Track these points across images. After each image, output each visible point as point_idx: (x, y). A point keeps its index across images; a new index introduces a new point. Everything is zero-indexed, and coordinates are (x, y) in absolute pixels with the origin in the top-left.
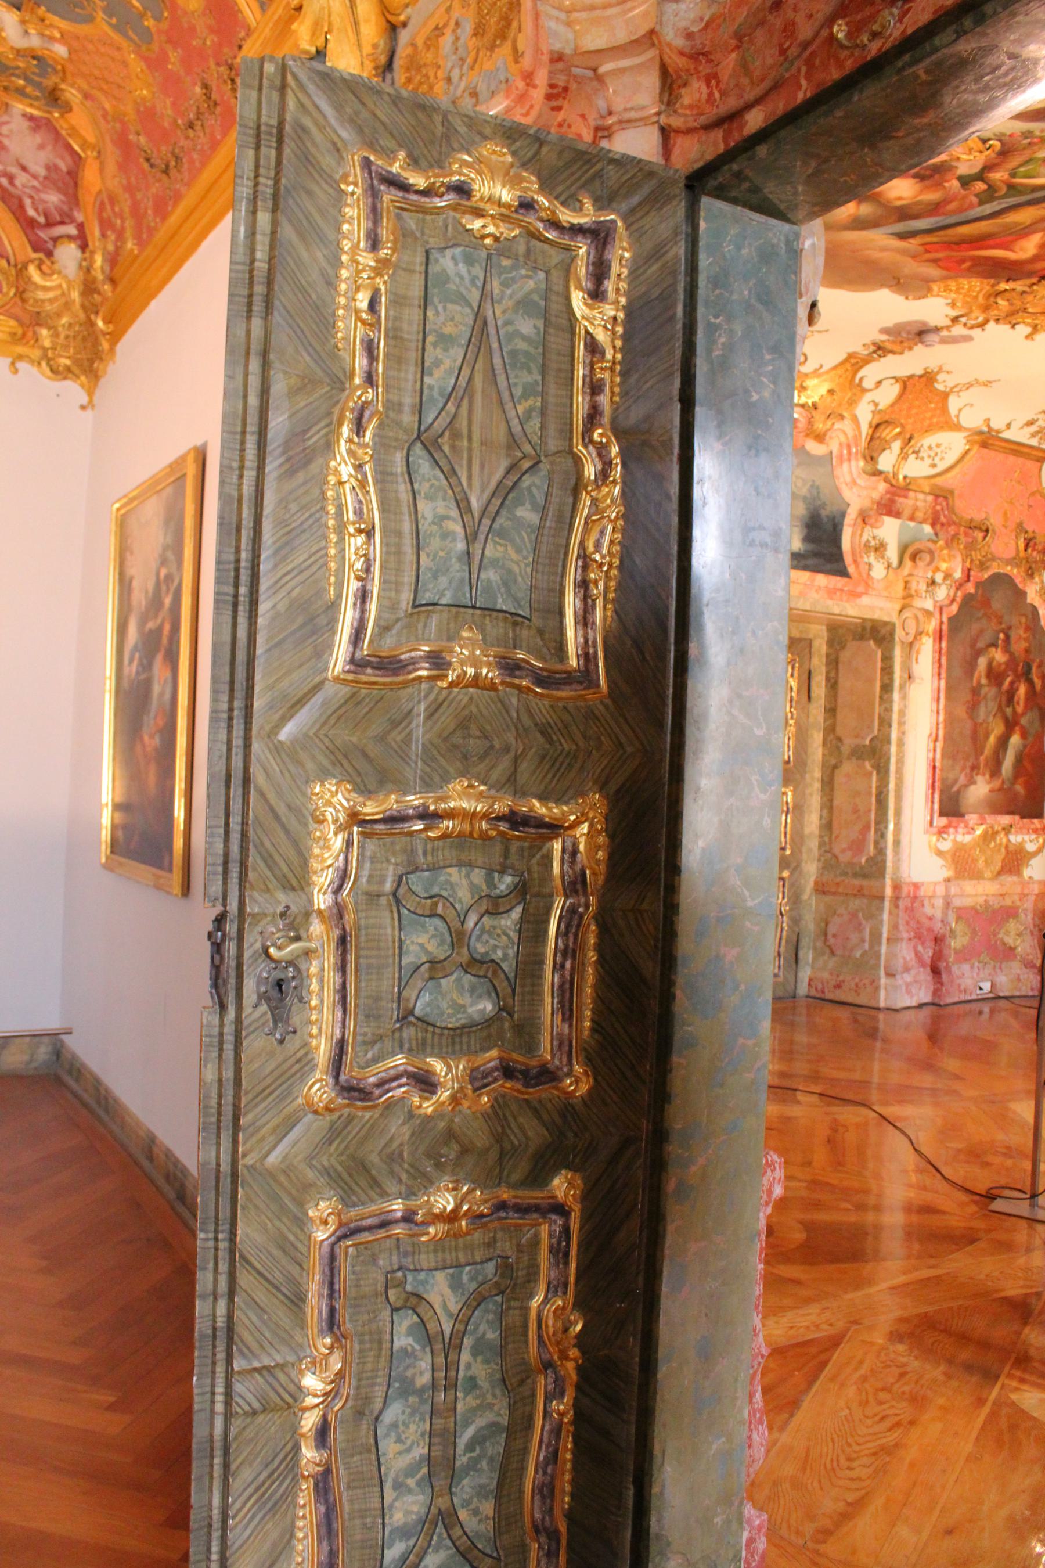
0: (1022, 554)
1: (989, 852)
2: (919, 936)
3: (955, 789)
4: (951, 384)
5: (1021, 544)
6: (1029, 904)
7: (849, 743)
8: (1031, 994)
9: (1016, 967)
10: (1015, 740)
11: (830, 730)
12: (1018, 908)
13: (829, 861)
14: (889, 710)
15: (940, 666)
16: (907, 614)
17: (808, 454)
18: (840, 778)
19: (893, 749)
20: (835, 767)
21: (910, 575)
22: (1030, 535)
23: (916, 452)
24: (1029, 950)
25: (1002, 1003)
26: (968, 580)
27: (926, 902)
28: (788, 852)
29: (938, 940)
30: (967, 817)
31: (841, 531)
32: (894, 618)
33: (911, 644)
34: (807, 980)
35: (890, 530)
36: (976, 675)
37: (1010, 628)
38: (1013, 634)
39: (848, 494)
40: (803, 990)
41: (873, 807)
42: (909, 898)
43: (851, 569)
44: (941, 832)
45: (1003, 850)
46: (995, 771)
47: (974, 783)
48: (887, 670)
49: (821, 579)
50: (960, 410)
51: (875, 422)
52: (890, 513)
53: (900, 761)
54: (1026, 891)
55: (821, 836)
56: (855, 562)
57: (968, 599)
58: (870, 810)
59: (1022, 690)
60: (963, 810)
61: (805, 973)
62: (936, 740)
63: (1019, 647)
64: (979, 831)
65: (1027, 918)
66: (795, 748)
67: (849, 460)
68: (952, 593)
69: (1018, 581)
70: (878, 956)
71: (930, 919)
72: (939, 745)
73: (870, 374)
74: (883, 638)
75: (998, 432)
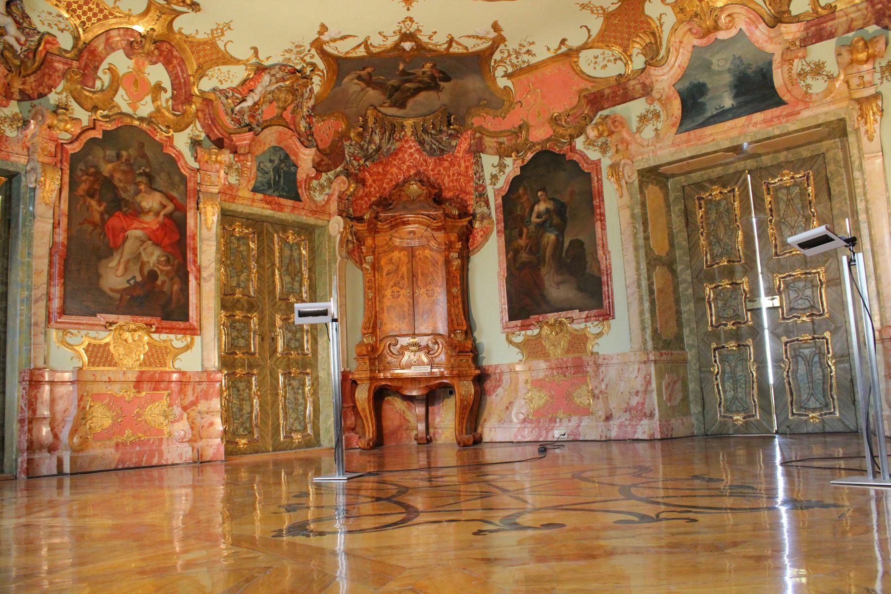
17: (723, 41)
31: (772, 75)
32: (843, 116)
39: (769, 48)
43: (785, 98)
49: (758, 117)
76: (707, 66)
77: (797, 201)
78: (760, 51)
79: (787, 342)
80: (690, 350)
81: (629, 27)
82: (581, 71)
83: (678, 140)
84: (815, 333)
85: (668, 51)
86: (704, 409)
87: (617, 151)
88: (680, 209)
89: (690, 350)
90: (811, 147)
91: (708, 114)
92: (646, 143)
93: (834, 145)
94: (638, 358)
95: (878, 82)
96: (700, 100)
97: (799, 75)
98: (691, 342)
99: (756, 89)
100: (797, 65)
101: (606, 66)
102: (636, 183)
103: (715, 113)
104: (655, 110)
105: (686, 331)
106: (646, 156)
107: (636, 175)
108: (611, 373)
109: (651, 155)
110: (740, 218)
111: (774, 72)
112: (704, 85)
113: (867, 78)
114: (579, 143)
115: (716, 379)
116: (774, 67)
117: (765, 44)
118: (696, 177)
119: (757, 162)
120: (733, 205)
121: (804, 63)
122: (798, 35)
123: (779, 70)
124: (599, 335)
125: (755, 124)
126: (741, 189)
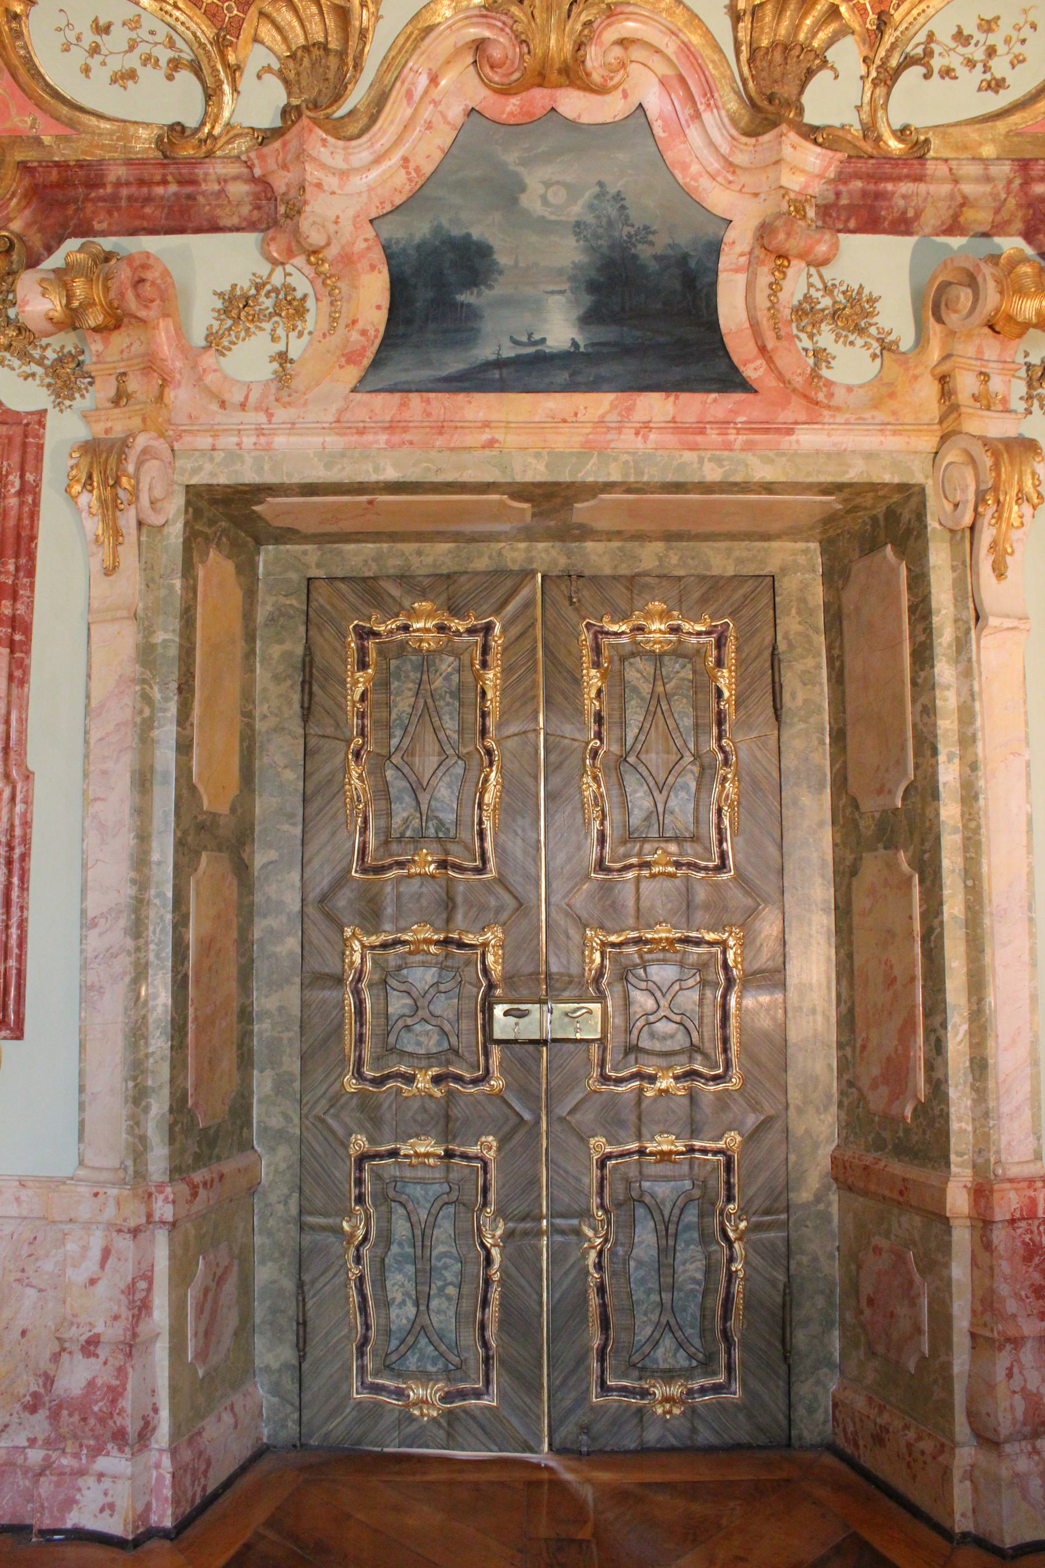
16: (952, 455)
17: (573, 125)
20: (854, 872)
21: (946, 357)
31: (714, 284)
32: (918, 478)
35: (878, 266)
39: (719, 199)
41: (919, 971)
43: (753, 371)
48: (921, 611)
49: (655, 406)
55: (840, 1046)
58: (913, 979)
67: (697, 115)
76: (506, 193)
78: (690, 198)
79: (609, 1157)
80: (272, 1150)
82: (29, 61)
83: (360, 414)
84: (694, 1133)
85: (379, 101)
86: (302, 1359)
87: (120, 398)
88: (287, 656)
89: (272, 1150)
90: (740, 549)
91: (486, 352)
92: (238, 397)
93: (802, 560)
94: (110, 1212)
95: (1021, 406)
96: (463, 297)
97: (799, 312)
98: (276, 1122)
99: (657, 316)
100: (797, 284)
101: (131, 75)
102: (176, 532)
103: (509, 352)
104: (289, 289)
105: (262, 1083)
106: (229, 441)
107: (179, 501)
110: (499, 726)
111: (722, 277)
112: (484, 251)
113: (996, 384)
115: (358, 1260)
116: (725, 261)
117: (705, 182)
118: (358, 556)
119: (569, 555)
120: (478, 677)
121: (815, 280)
122: (816, 188)
123: (741, 279)
125: (644, 428)
126: (514, 631)
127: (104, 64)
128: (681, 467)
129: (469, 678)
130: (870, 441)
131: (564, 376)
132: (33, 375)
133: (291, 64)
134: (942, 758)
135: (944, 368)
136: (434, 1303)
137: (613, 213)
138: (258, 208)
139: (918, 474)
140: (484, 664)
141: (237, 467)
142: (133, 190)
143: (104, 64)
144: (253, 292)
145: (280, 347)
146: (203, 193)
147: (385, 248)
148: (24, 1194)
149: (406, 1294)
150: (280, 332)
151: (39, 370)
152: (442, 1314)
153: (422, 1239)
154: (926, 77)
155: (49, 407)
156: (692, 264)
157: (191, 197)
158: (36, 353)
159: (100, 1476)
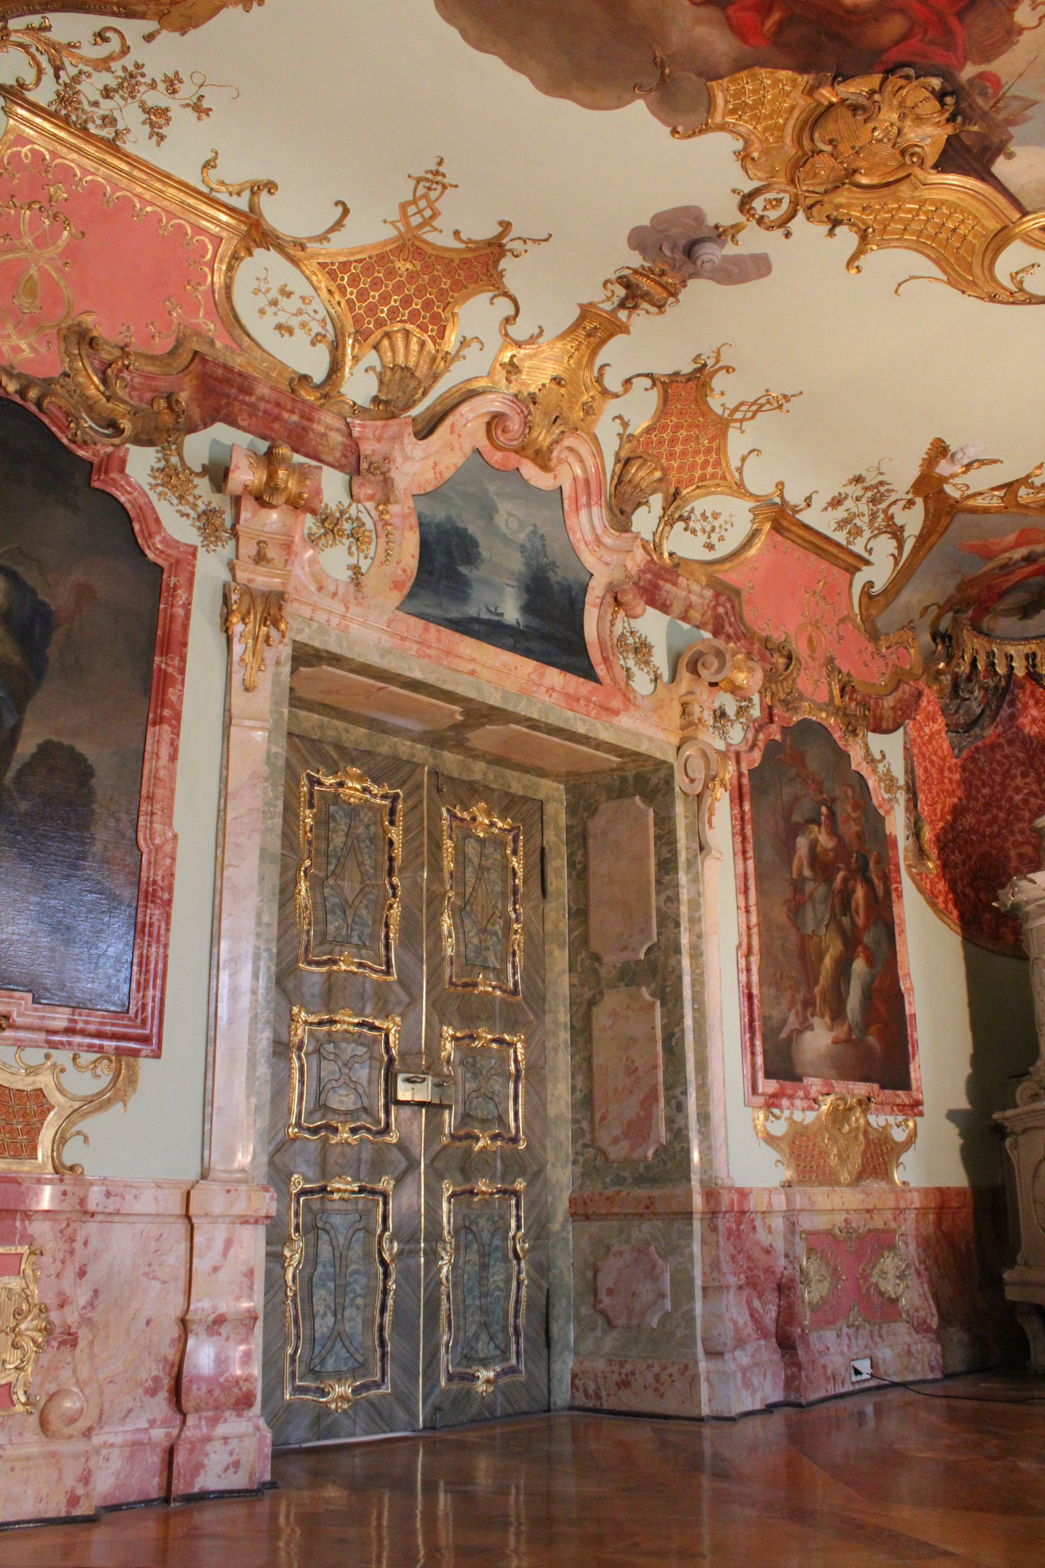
0: (837, 701)
1: (842, 1142)
2: (752, 1283)
3: (783, 1035)
4: (731, 404)
5: (836, 692)
6: (908, 1225)
7: (612, 959)
8: (930, 1376)
9: (902, 1332)
10: (859, 965)
11: (580, 943)
12: (894, 1231)
13: (592, 1162)
14: (674, 899)
15: (744, 839)
16: (689, 751)
17: (525, 482)
18: (601, 1017)
19: (686, 962)
20: (592, 1003)
21: (690, 693)
22: (846, 679)
23: (686, 520)
24: (917, 1302)
25: (895, 1396)
26: (771, 720)
27: (758, 1223)
28: (522, 1146)
29: (784, 1288)
30: (807, 1081)
33: (699, 797)
34: (568, 1378)
36: (796, 862)
37: (834, 800)
38: (838, 808)
39: (589, 560)
40: (562, 1395)
41: (660, 1062)
42: (731, 1212)
43: (601, 670)
44: (771, 1102)
45: (861, 1137)
46: (838, 1014)
47: (810, 1028)
48: (666, 838)
49: (554, 677)
50: (744, 459)
51: (623, 455)
52: (652, 602)
53: (699, 982)
54: (902, 1205)
55: (575, 1121)
56: (606, 660)
57: (772, 750)
58: (655, 1067)
59: (860, 893)
60: (799, 1070)
61: (565, 1365)
62: (749, 953)
63: (849, 829)
64: (826, 1104)
65: (910, 1249)
66: (525, 969)
67: (589, 506)
68: (750, 736)
69: (837, 736)
70: (690, 1321)
71: (768, 1252)
72: (755, 960)
73: (619, 357)
74: (656, 790)
75: (796, 510)
76: (488, 512)
77: (494, 876)
81: (406, 302)
90: (528, 778)
91: (472, 611)
92: (332, 588)
103: (485, 616)
106: (321, 617)
108: (119, 1247)
109: (335, 621)
111: (587, 607)
112: (474, 543)
114: (141, 463)
117: (582, 546)
119: (435, 757)
123: (596, 611)
124: (97, 1103)
126: (410, 803)
127: (275, 314)
128: (567, 719)
129: (380, 831)
130: (651, 731)
131: (510, 642)
132: (188, 515)
133: (389, 373)
134: (682, 929)
135: (688, 699)
136: (347, 1313)
137: (540, 548)
138: (345, 456)
139: (671, 757)
140: (392, 823)
141: (326, 638)
142: (269, 407)
143: (275, 314)
144: (338, 515)
145: (353, 561)
146: (313, 431)
147: (419, 518)
148: (161, 1193)
149: (328, 1307)
150: (354, 549)
151: (193, 514)
152: (354, 1323)
153: (340, 1259)
154: (686, 529)
155: (199, 545)
156: (574, 593)
157: (304, 429)
158: (191, 499)
159: (226, 1439)
